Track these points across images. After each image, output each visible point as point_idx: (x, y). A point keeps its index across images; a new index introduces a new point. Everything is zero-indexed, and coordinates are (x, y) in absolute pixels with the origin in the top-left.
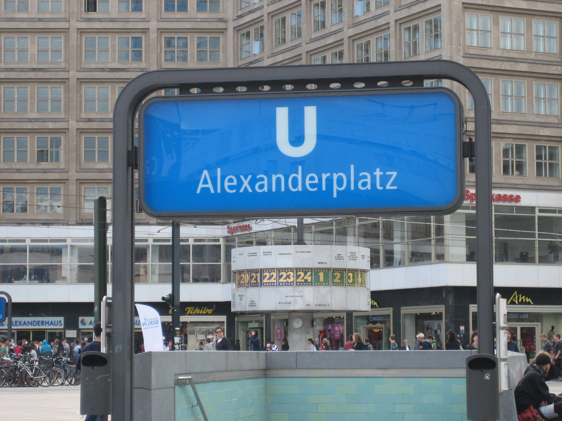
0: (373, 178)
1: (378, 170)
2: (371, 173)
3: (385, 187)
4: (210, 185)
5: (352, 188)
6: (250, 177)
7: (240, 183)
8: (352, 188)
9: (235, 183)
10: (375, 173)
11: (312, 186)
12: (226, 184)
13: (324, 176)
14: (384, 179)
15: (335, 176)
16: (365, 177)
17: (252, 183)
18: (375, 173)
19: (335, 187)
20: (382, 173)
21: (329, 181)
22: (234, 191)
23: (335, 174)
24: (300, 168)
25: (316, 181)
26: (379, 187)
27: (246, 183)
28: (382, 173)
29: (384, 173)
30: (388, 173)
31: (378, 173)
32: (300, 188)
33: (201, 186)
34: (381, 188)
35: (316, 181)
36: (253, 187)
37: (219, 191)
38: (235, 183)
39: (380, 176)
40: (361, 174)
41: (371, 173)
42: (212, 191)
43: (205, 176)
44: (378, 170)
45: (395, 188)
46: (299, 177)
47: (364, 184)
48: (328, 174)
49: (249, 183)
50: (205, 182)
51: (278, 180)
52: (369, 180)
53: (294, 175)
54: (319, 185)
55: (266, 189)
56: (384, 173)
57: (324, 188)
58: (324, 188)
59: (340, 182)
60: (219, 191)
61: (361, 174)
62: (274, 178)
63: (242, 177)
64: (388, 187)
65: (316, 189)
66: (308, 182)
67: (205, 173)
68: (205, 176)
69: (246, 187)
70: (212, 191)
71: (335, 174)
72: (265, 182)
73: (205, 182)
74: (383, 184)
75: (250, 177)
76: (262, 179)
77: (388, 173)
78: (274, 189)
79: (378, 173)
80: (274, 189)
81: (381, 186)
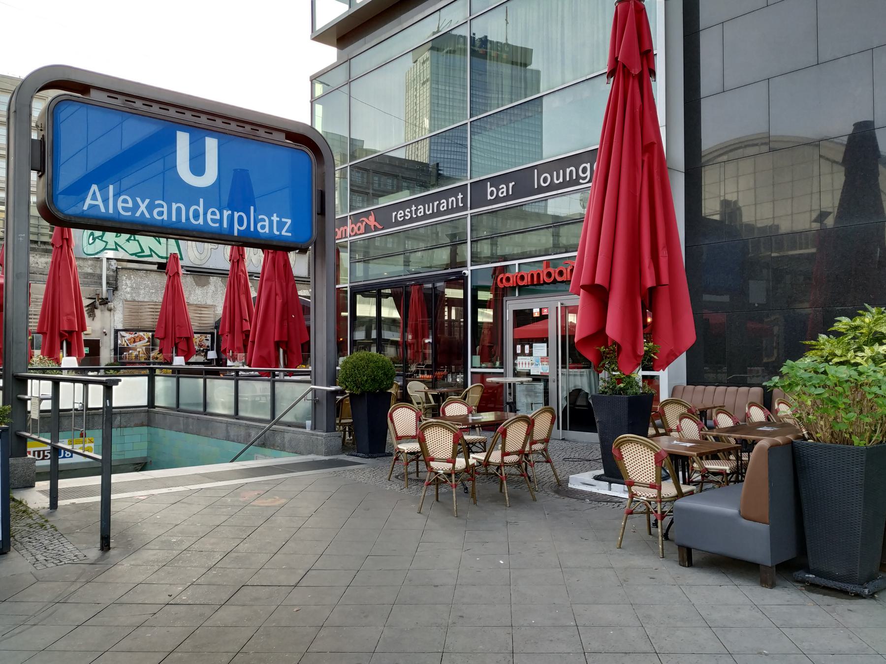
0: (271, 222)
1: (275, 215)
2: (269, 216)
3: (281, 233)
4: (99, 202)
5: (252, 229)
6: (147, 201)
7: (136, 207)
8: (252, 229)
9: (130, 205)
10: (272, 218)
11: (213, 221)
12: (120, 205)
13: (226, 213)
14: (281, 225)
15: (236, 215)
16: (264, 220)
17: (150, 208)
18: (272, 218)
19: (236, 226)
20: (278, 219)
21: (231, 219)
22: (129, 214)
23: (235, 213)
24: (201, 201)
25: (218, 217)
27: (143, 207)
28: (278, 219)
29: (281, 219)
30: (284, 220)
33: (89, 201)
34: (278, 233)
35: (218, 217)
36: (151, 213)
37: (111, 211)
38: (130, 205)
39: (277, 221)
40: (260, 217)
41: (269, 216)
42: (103, 210)
43: (94, 191)
44: (275, 215)
45: (290, 234)
47: (263, 227)
48: (230, 212)
50: (94, 198)
51: (179, 210)
52: (267, 223)
53: (194, 207)
54: (221, 221)
55: (165, 217)
56: (281, 219)
57: (225, 225)
58: (225, 225)
59: (241, 222)
60: (111, 211)
61: (260, 217)
62: (174, 206)
63: (139, 200)
64: (284, 233)
65: (217, 225)
66: (209, 216)
67: (94, 187)
68: (94, 191)
69: (143, 212)
70: (103, 210)
71: (235, 213)
72: (165, 210)
73: (94, 198)
74: (280, 228)
75: (147, 201)
77: (284, 220)
78: (174, 219)
79: (275, 218)
80: (174, 219)
81: (277, 231)
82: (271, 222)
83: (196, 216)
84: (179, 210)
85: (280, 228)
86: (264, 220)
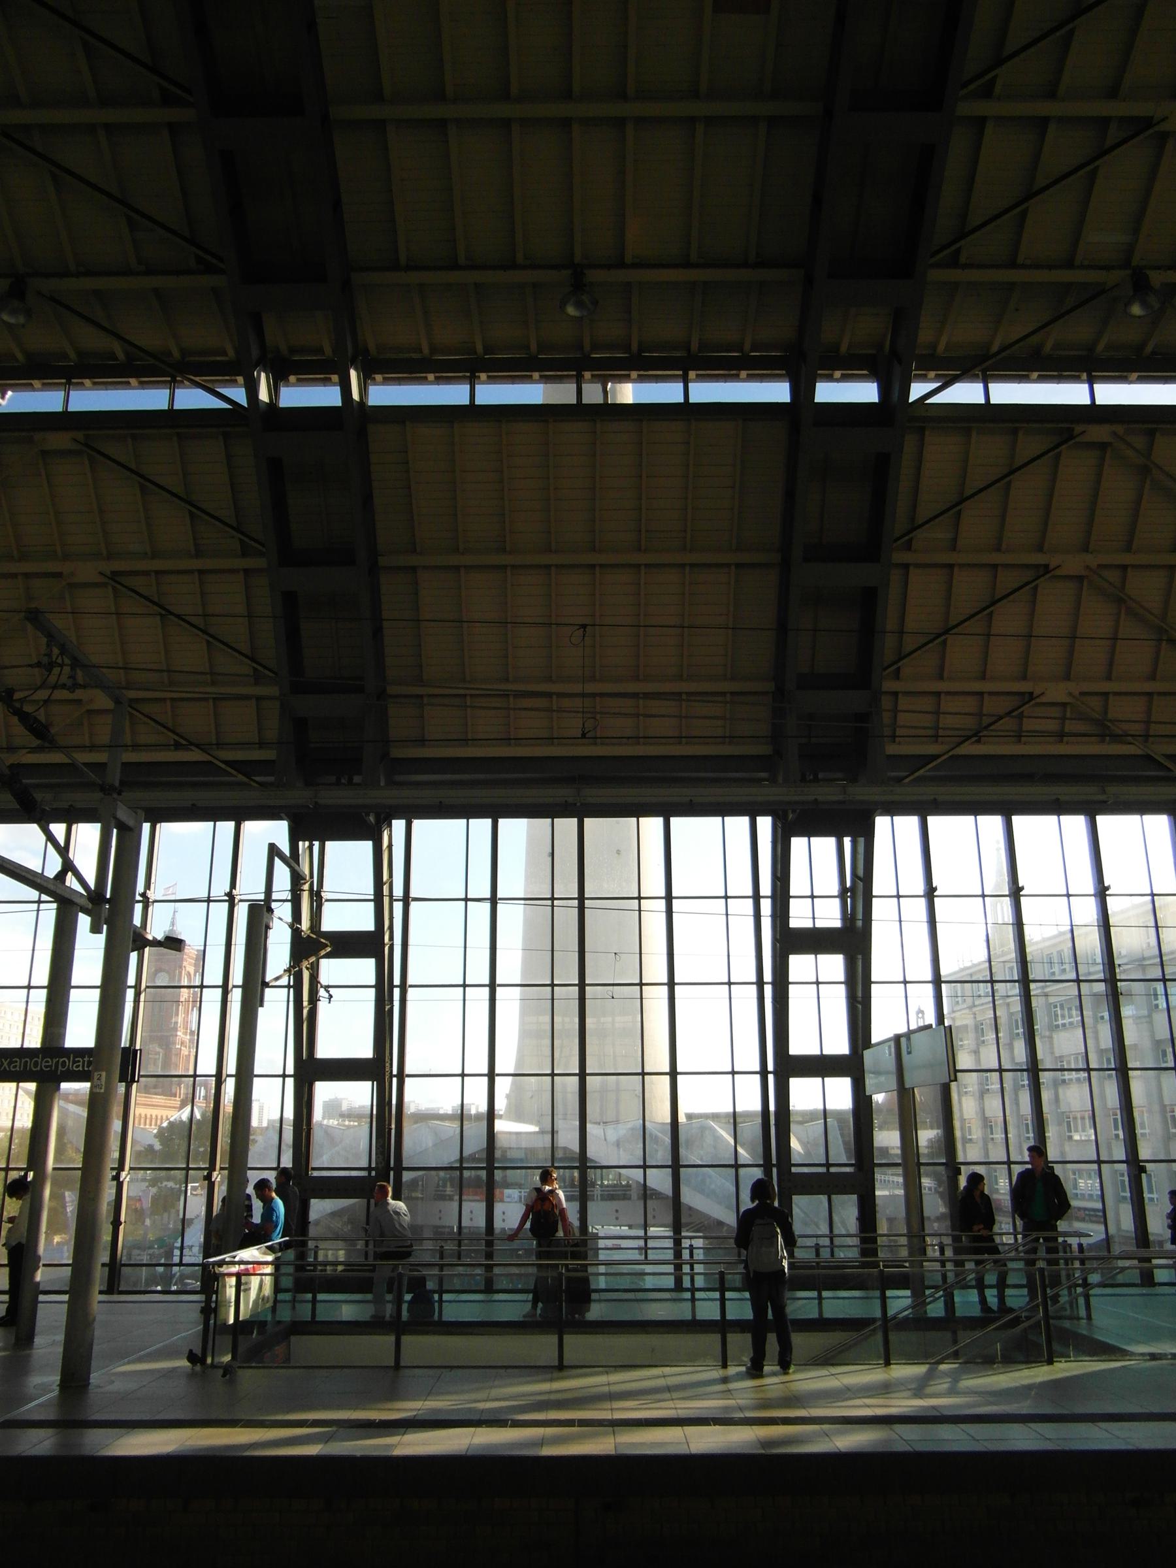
0: (84, 1062)
17: (9, 1065)
19: (60, 1068)
26: (86, 1069)
31: (86, 1059)
32: (39, 1068)
35: (50, 1064)
36: (9, 1068)
46: (40, 1061)
49: (8, 1064)
52: (81, 1064)
53: (36, 1059)
62: (23, 1061)
66: (44, 1064)
72: (18, 1064)
74: (88, 1067)
76: (17, 1062)
82: (84, 1062)
83: (36, 1064)
84: (27, 1061)
85: (88, 1067)
86: (79, 1061)
